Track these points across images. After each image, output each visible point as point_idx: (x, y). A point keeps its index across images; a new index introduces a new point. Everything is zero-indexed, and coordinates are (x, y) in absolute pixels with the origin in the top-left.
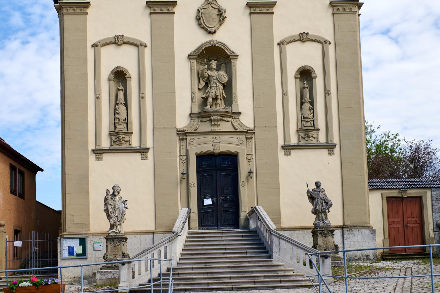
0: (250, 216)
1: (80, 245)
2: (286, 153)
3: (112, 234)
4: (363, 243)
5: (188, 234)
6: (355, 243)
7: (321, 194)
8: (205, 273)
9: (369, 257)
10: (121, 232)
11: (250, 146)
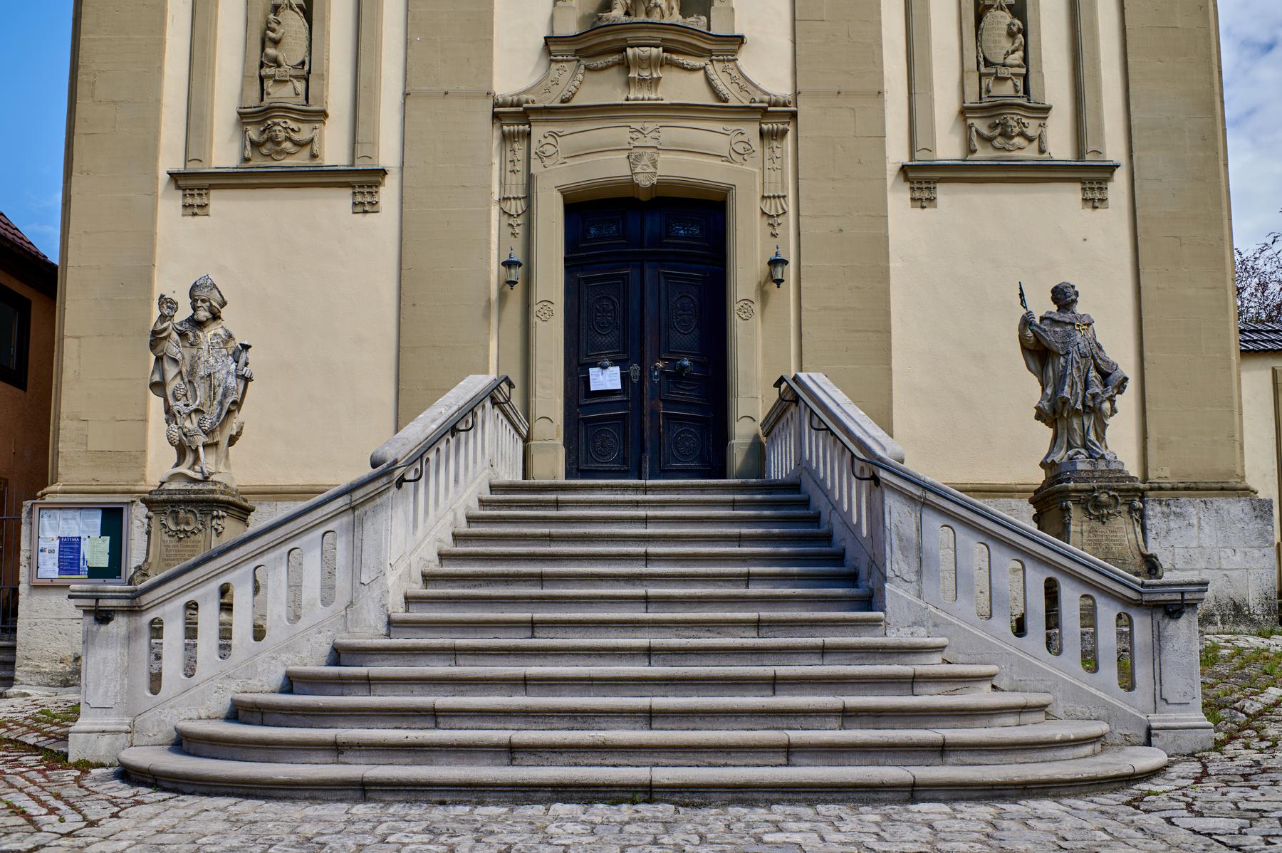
0: (773, 434)
1: (103, 533)
2: (917, 195)
3: (174, 486)
4: (1222, 554)
5: (491, 491)
6: (1191, 552)
7: (1079, 336)
8: (516, 679)
9: (1247, 612)
10: (213, 478)
11: (775, 166)
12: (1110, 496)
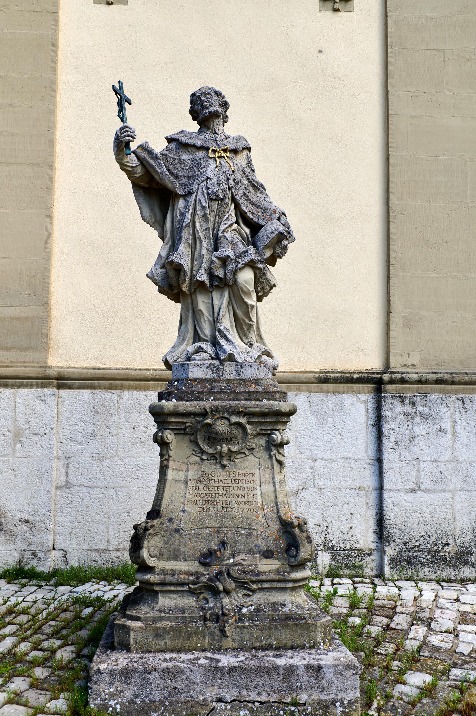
6: (442, 467)
7: (212, 167)
12: (231, 424)
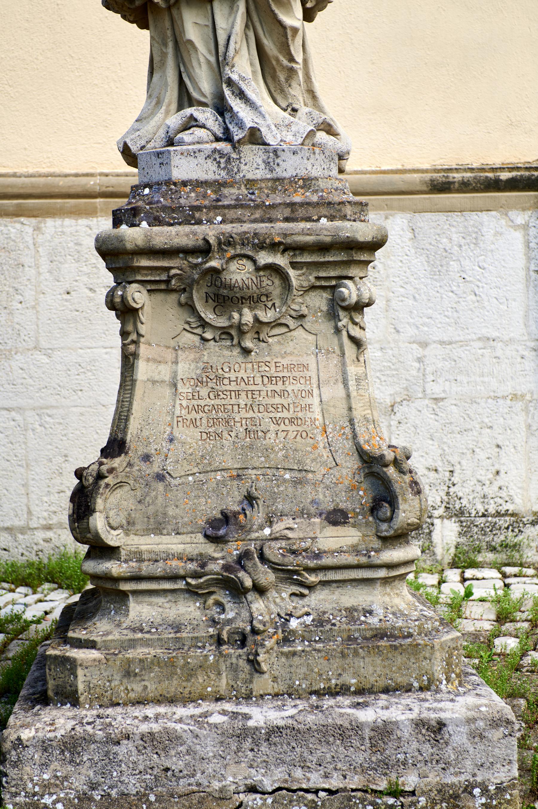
12: (258, 269)
